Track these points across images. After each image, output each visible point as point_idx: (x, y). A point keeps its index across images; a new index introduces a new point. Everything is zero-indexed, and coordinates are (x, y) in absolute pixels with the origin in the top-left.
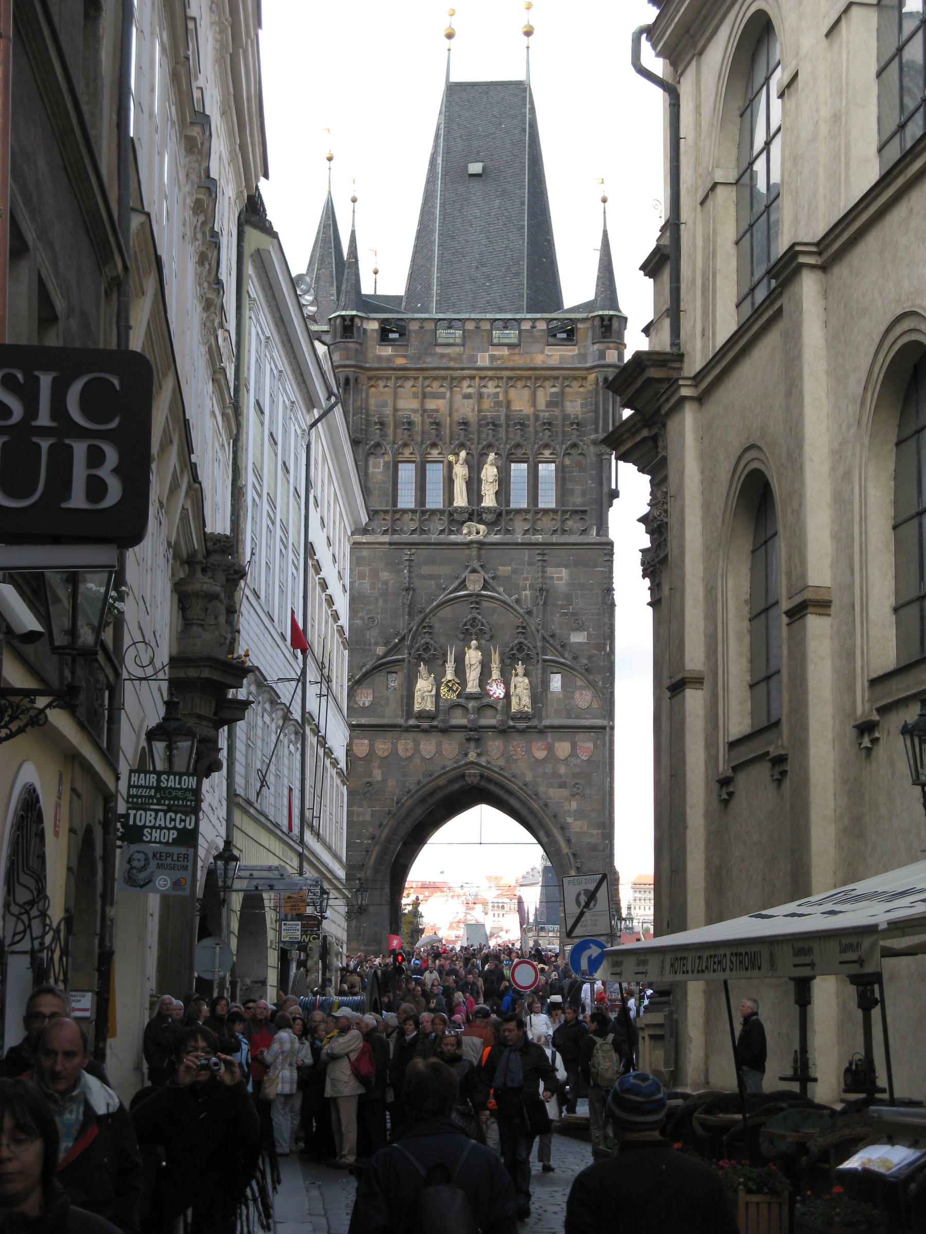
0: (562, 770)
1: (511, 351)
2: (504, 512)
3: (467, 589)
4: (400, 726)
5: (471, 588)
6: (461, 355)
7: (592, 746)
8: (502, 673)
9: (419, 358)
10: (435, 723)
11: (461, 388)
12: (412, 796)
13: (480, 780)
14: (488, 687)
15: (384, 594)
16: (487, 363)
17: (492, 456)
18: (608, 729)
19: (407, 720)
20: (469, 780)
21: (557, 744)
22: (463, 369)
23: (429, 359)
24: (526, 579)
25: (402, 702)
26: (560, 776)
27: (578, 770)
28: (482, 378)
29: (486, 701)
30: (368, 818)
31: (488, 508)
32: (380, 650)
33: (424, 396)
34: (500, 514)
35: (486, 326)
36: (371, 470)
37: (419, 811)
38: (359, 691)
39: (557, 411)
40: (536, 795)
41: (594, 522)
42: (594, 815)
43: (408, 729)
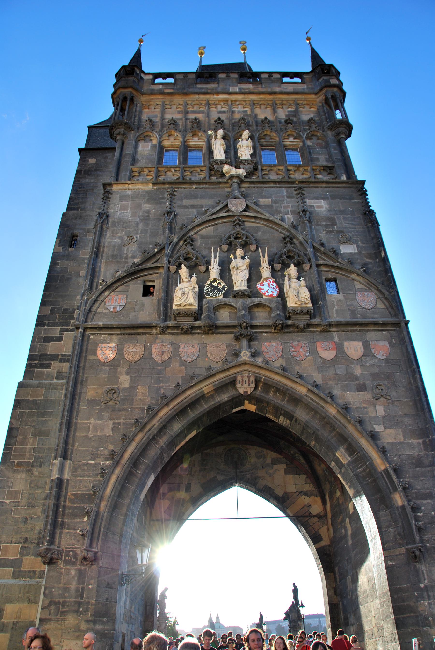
0: (358, 371)
1: (255, 86)
2: (259, 167)
3: (228, 211)
4: (156, 327)
5: (233, 209)
6: (216, 88)
7: (388, 346)
9: (184, 89)
10: (197, 323)
12: (167, 405)
13: (256, 388)
14: (259, 286)
15: (146, 219)
17: (246, 133)
18: (403, 324)
19: (165, 320)
21: (346, 344)
22: (218, 93)
23: (191, 90)
24: (288, 207)
26: (356, 378)
27: (376, 370)
29: (256, 300)
30: (108, 432)
31: (245, 160)
32: (136, 260)
34: (256, 169)
37: (177, 427)
40: (332, 397)
41: (343, 172)
42: (408, 421)
43: (164, 330)
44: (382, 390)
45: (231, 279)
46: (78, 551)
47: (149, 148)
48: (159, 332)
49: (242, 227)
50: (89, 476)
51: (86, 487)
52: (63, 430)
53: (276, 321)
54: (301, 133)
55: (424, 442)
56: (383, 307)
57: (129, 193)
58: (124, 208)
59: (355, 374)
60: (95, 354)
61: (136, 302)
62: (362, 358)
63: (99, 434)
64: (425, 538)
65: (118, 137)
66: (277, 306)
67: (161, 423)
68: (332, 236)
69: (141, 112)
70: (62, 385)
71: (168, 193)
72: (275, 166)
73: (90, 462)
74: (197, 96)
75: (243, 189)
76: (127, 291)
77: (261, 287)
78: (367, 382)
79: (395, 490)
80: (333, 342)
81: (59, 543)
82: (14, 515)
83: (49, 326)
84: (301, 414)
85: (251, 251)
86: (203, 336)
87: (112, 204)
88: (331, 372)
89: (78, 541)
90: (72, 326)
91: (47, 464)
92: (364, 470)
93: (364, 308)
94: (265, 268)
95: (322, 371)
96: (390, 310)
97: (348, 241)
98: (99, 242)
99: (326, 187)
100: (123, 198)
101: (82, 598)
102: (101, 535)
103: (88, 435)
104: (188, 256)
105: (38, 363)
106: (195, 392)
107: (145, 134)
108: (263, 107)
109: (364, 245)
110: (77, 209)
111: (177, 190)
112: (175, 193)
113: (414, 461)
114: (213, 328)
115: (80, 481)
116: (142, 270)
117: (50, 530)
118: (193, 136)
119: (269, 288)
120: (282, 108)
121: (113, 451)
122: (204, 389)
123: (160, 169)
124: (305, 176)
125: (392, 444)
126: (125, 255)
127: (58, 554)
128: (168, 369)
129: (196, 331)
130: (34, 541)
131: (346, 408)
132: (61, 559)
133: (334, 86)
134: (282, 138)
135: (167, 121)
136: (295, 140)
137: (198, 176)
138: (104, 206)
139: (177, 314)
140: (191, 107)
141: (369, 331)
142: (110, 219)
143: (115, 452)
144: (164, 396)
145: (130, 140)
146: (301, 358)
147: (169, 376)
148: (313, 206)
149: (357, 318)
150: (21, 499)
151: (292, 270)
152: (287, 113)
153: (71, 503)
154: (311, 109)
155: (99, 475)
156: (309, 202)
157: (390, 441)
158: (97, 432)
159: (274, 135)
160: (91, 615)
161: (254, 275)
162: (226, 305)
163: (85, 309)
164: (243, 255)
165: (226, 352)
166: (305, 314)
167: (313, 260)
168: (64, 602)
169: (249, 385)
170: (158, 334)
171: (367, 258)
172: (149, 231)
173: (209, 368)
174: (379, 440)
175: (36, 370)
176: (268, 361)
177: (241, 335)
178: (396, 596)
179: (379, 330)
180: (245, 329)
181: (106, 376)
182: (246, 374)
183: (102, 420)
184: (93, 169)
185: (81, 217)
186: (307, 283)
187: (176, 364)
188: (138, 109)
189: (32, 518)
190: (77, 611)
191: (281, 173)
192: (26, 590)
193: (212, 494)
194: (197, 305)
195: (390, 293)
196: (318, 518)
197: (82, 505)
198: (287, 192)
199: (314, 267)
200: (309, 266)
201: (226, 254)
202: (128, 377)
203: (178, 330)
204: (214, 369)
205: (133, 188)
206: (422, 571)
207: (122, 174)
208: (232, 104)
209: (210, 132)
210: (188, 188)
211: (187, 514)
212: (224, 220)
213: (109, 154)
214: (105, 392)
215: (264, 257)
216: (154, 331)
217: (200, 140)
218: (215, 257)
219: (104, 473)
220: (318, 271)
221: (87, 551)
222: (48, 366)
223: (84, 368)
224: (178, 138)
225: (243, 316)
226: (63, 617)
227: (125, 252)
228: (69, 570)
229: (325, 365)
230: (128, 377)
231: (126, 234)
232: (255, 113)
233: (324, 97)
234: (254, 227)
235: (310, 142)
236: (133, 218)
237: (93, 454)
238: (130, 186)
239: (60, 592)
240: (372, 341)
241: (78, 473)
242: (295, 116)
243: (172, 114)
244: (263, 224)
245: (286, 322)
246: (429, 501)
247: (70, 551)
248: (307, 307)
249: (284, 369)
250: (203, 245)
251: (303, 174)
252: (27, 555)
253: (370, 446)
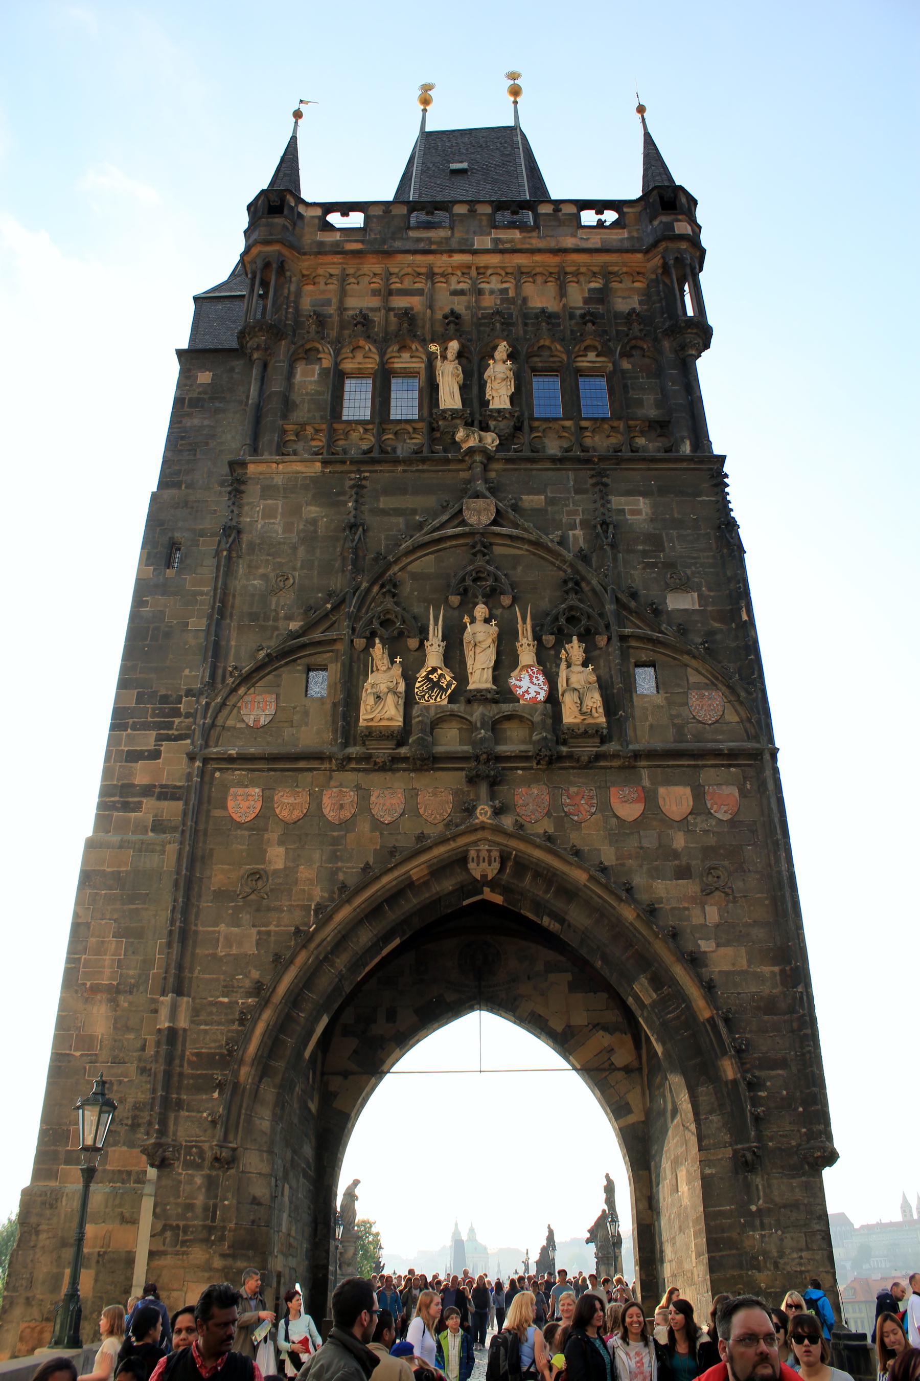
0: (679, 841)
1: (525, 234)
2: (526, 423)
4: (330, 758)
6: (447, 239)
7: (737, 795)
8: (540, 660)
9: (384, 241)
11: (450, 285)
12: (348, 901)
14: (513, 681)
15: (310, 538)
16: (489, 246)
18: (767, 756)
19: (346, 745)
20: (476, 870)
21: (662, 791)
22: (451, 252)
24: (575, 512)
25: (334, 715)
26: (676, 855)
27: (711, 841)
28: (481, 271)
29: (507, 708)
30: (250, 948)
31: (499, 411)
32: (294, 626)
33: (390, 293)
35: (488, 209)
36: (298, 378)
37: (365, 937)
38: (247, 698)
39: (601, 308)
40: (629, 890)
41: (685, 434)
42: (758, 933)
43: (344, 764)
44: (718, 877)
45: (463, 663)
46: (206, 1146)
47: (316, 376)
48: (334, 768)
49: (487, 557)
50: (219, 1024)
51: (215, 1041)
52: (175, 945)
53: (540, 750)
54: (611, 344)
55: (782, 971)
56: (737, 719)
57: (278, 480)
58: (269, 513)
59: (674, 846)
60: (225, 808)
61: (294, 708)
62: (690, 818)
63: (234, 952)
64: (768, 1133)
65: (256, 356)
66: (543, 721)
67: (339, 932)
68: (654, 575)
69: (299, 294)
70: (163, 845)
71: (352, 482)
72: (556, 419)
73: (221, 999)
74: (410, 258)
75: (493, 475)
76: (278, 686)
77: (518, 683)
78: (694, 863)
79: (724, 1053)
80: (640, 788)
81: (175, 1134)
82: (89, 1076)
83: (135, 730)
84: (577, 917)
85: (503, 607)
86: (413, 775)
87: (248, 504)
88: (632, 844)
89: (206, 1131)
90: (177, 730)
91: (142, 989)
92: (678, 1017)
93: (700, 722)
94: (525, 646)
95: (617, 841)
96: (748, 725)
97: (684, 586)
98: (225, 586)
99: (649, 469)
100: (268, 491)
101: (213, 1220)
102: (242, 1121)
103: (215, 954)
104: (388, 616)
105: (118, 802)
106: (396, 878)
107: (308, 347)
108: (539, 279)
109: (712, 594)
110: (178, 485)
111: (367, 474)
112: (364, 482)
113: (762, 1004)
114: (429, 762)
115: (206, 1031)
116: (304, 646)
117: (160, 1113)
118: (399, 351)
119: (531, 685)
120: (577, 283)
121: (258, 982)
122: (411, 873)
123: (336, 426)
124: (613, 440)
125: (727, 973)
126: (273, 614)
127: (173, 1151)
128: (351, 836)
129: (400, 766)
130: (125, 1122)
131: (651, 912)
132: (178, 1159)
133: (682, 237)
134: (573, 357)
135: (351, 313)
136: (599, 359)
137: (408, 441)
138: (232, 512)
139: (366, 736)
140: (397, 280)
141: (705, 766)
142: (245, 538)
143: (263, 984)
144: (343, 887)
145: (280, 362)
146: (581, 816)
147: (353, 849)
148: (623, 510)
149: (687, 742)
150: (101, 1049)
151: (575, 649)
152: (587, 295)
153: (192, 1069)
154: (637, 285)
155: (237, 1023)
156: (616, 501)
157: (725, 968)
158: (231, 947)
159: (559, 347)
160: (229, 1247)
161: (505, 661)
162: (453, 716)
163: (204, 723)
164: (487, 616)
165: (451, 805)
166: (592, 736)
167: (614, 628)
168: (186, 1230)
170: (335, 771)
171: (715, 620)
172: (316, 563)
173: (421, 837)
174: (706, 966)
175: (115, 814)
176: (525, 823)
177: (478, 776)
178: (713, 1223)
179: (723, 765)
180: (485, 763)
181: (245, 847)
182: (484, 847)
183: (238, 926)
184: (206, 396)
185: (186, 504)
186: (603, 672)
187: (364, 827)
188: (293, 289)
189: (120, 1082)
190: (206, 1241)
191: (566, 434)
192: (117, 1201)
193: (436, 1025)
194: (401, 719)
195: (749, 693)
196: (626, 1073)
197: (210, 1072)
198: (575, 481)
199: (615, 639)
200: (605, 638)
201: (456, 613)
202: (281, 850)
203: (368, 763)
204: (430, 838)
205: (285, 471)
206: (757, 1186)
207: (265, 439)
208: (479, 274)
209: (434, 348)
210: (389, 472)
211: (389, 1062)
212: (454, 543)
213: (238, 363)
214: (242, 877)
215: (524, 621)
216: (326, 765)
217: (414, 360)
218: (436, 623)
219: (246, 1019)
220: (621, 648)
221: (221, 1147)
222: (137, 807)
223: (205, 834)
224: (372, 355)
225: (483, 740)
226: (185, 1249)
227: (273, 607)
228: (192, 1176)
229: (622, 830)
231: (273, 570)
232: (524, 294)
233: (661, 261)
234: (509, 555)
235: (628, 363)
236: (287, 535)
237: (225, 987)
238: (281, 466)
239: (180, 1210)
240: (709, 785)
241: (202, 1018)
242: (601, 301)
243: (361, 300)
244: (527, 550)
245: (558, 750)
246: (780, 1072)
247: (192, 1147)
248: (596, 724)
249: (549, 838)
250: (416, 593)
251: (608, 436)
252: (115, 1144)
253: (688, 978)
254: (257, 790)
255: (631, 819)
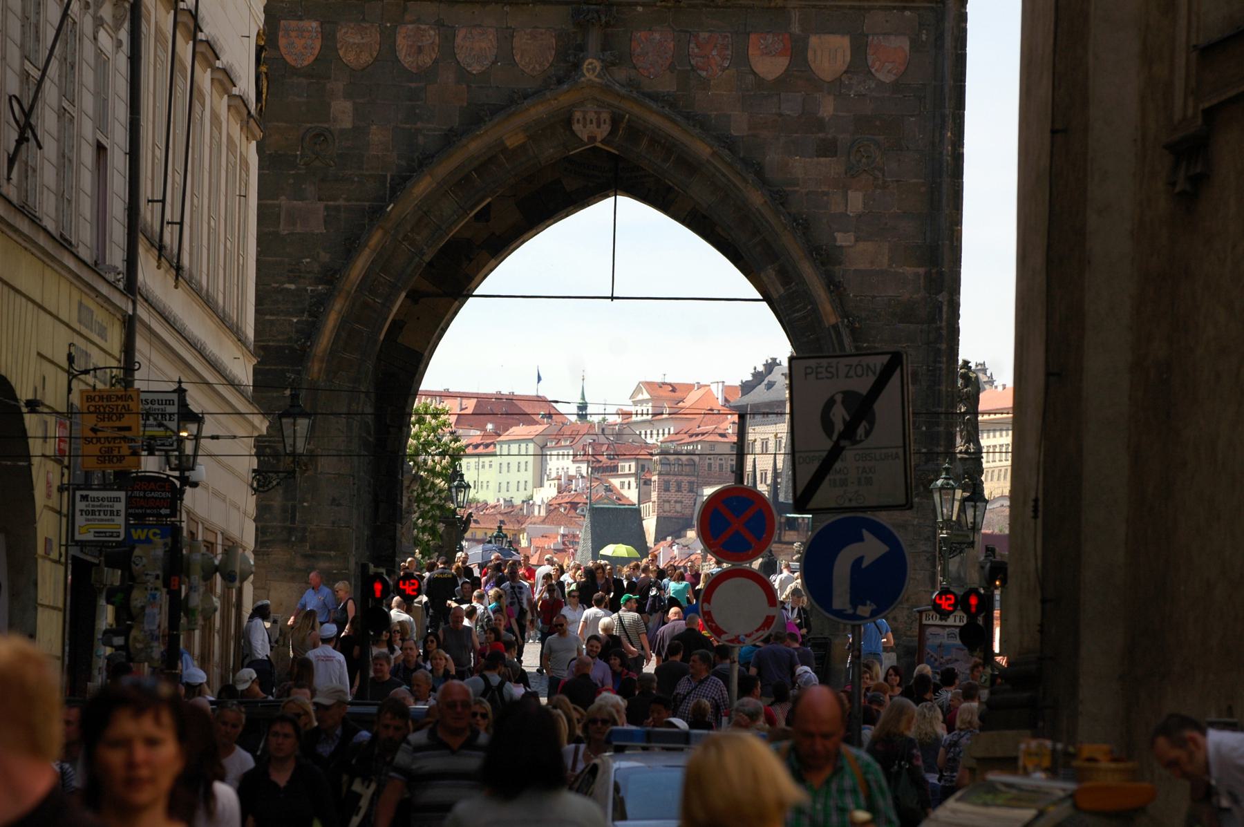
0: (827, 108)
7: (907, 48)
21: (814, 40)
26: (820, 125)
40: (759, 172)
59: (820, 114)
73: (287, 286)
86: (507, 8)
115: (272, 322)
131: (779, 198)
141: (871, 8)
157: (861, 267)
169: (599, 126)
179: (894, 8)
202: (348, 105)
230: (348, 105)
254: (314, 24)
255: (771, 77)
